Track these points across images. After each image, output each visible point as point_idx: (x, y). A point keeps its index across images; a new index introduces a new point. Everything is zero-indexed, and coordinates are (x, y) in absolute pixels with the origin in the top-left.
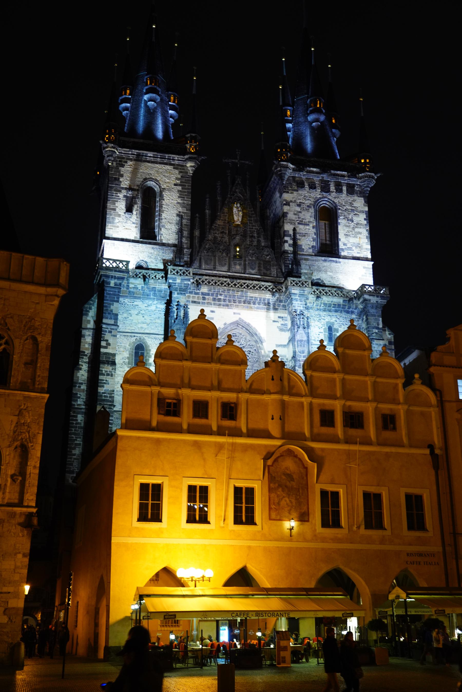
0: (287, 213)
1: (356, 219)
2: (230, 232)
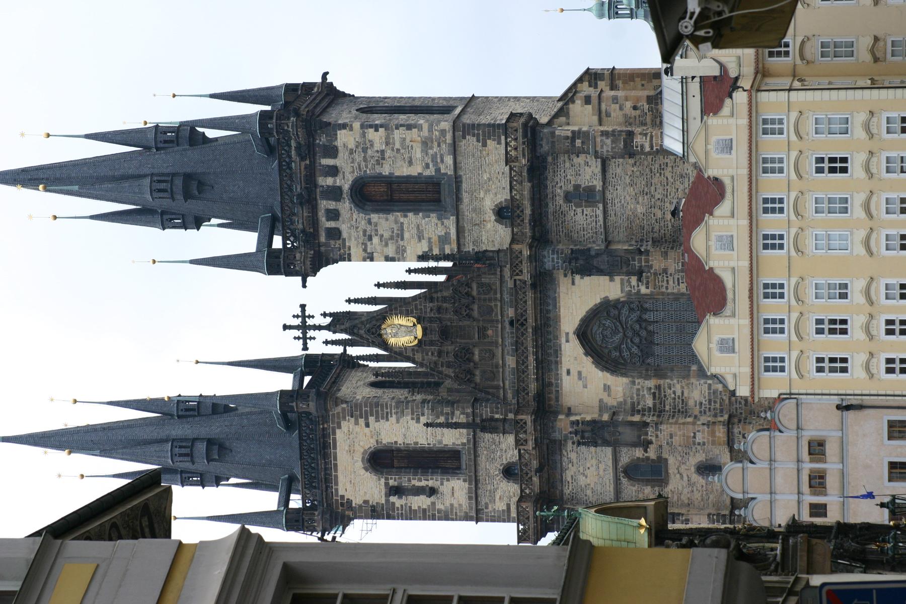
1: (378, 146)
2: (432, 343)
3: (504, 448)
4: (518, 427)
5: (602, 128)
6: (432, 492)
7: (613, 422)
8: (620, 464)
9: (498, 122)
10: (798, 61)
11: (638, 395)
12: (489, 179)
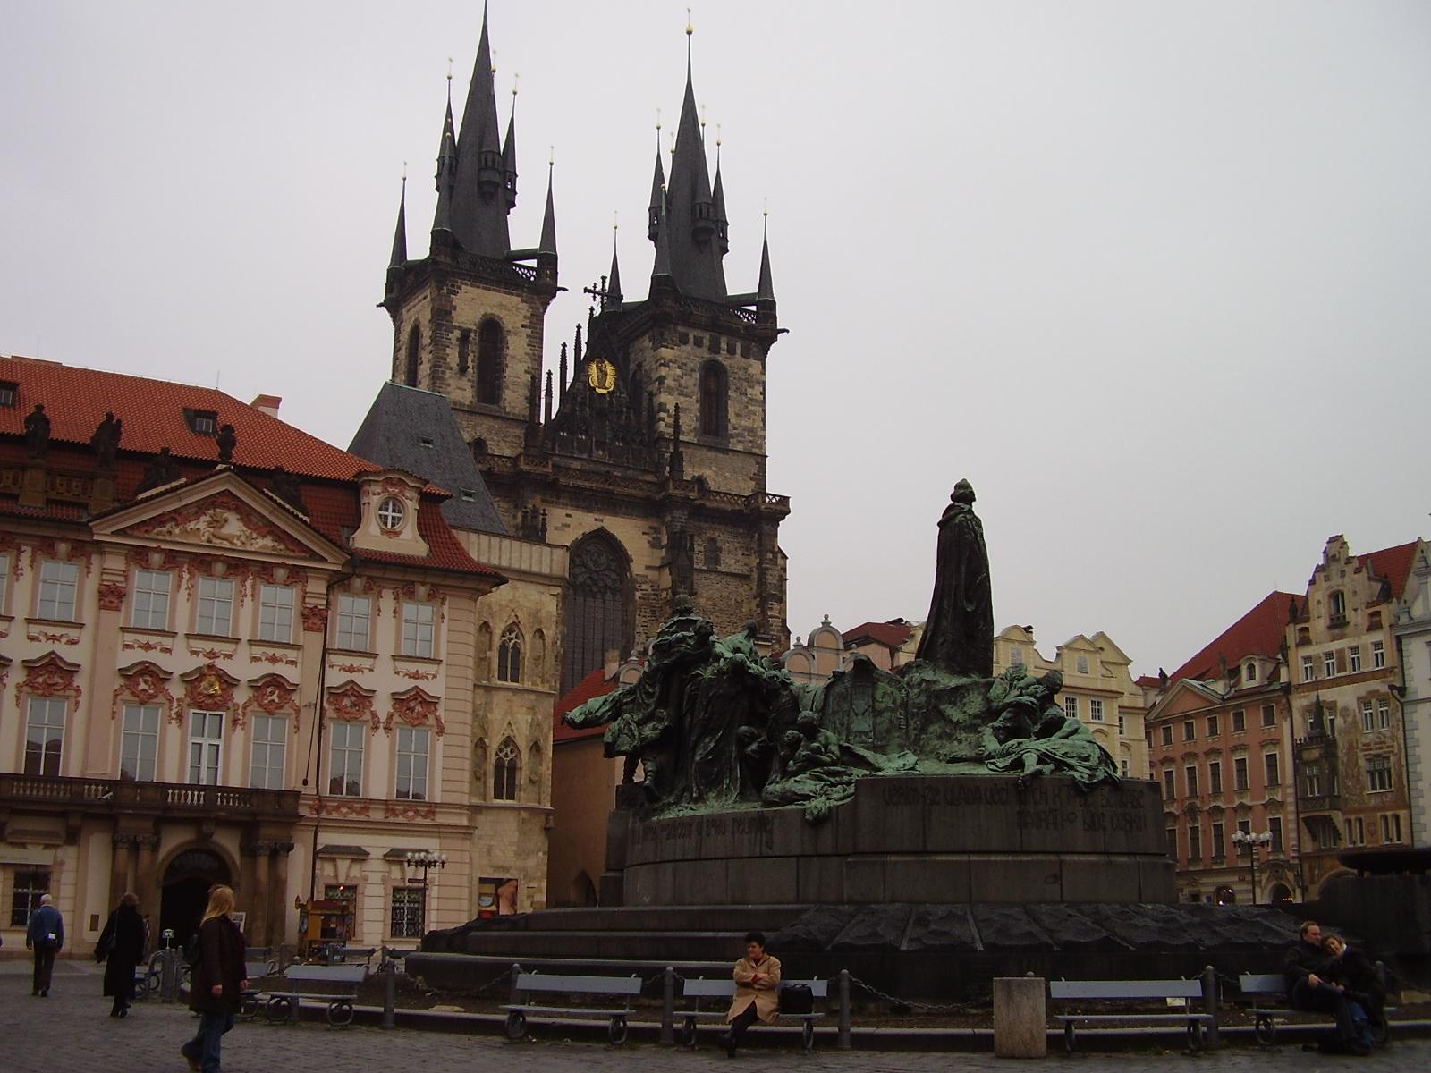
0: (664, 377)
12: (725, 477)
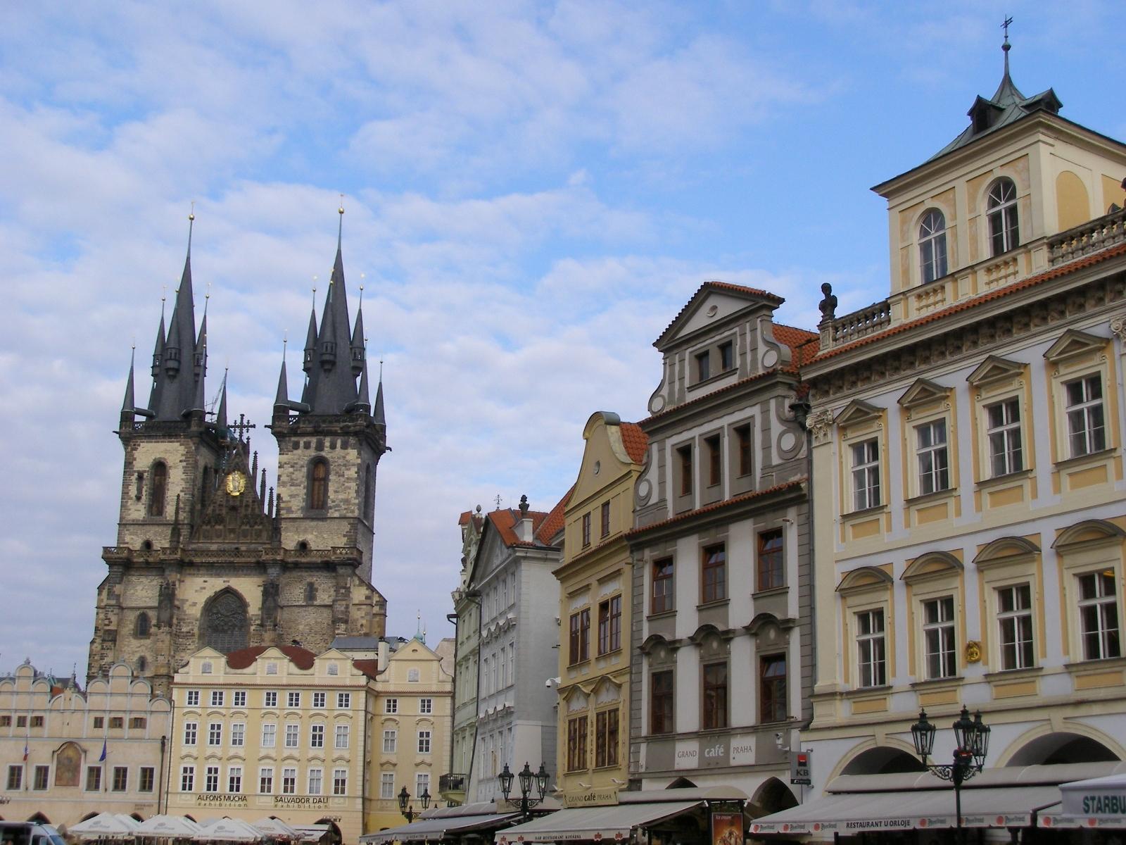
2: (228, 501)
3: (161, 541)
4: (174, 549)
5: (351, 605)
6: (139, 498)
7: (173, 606)
8: (148, 610)
9: (358, 545)
10: (384, 718)
11: (189, 623)
